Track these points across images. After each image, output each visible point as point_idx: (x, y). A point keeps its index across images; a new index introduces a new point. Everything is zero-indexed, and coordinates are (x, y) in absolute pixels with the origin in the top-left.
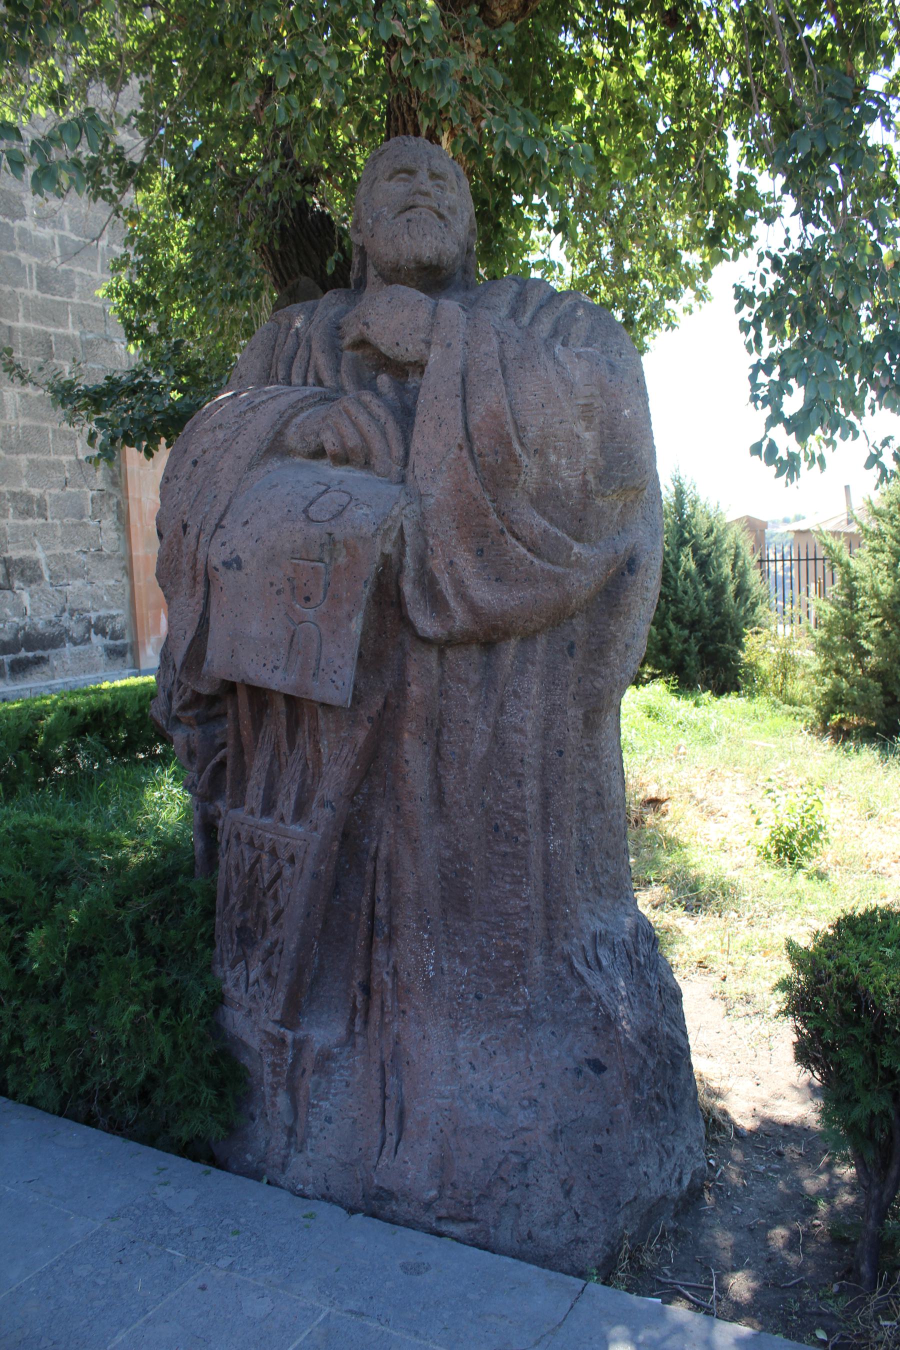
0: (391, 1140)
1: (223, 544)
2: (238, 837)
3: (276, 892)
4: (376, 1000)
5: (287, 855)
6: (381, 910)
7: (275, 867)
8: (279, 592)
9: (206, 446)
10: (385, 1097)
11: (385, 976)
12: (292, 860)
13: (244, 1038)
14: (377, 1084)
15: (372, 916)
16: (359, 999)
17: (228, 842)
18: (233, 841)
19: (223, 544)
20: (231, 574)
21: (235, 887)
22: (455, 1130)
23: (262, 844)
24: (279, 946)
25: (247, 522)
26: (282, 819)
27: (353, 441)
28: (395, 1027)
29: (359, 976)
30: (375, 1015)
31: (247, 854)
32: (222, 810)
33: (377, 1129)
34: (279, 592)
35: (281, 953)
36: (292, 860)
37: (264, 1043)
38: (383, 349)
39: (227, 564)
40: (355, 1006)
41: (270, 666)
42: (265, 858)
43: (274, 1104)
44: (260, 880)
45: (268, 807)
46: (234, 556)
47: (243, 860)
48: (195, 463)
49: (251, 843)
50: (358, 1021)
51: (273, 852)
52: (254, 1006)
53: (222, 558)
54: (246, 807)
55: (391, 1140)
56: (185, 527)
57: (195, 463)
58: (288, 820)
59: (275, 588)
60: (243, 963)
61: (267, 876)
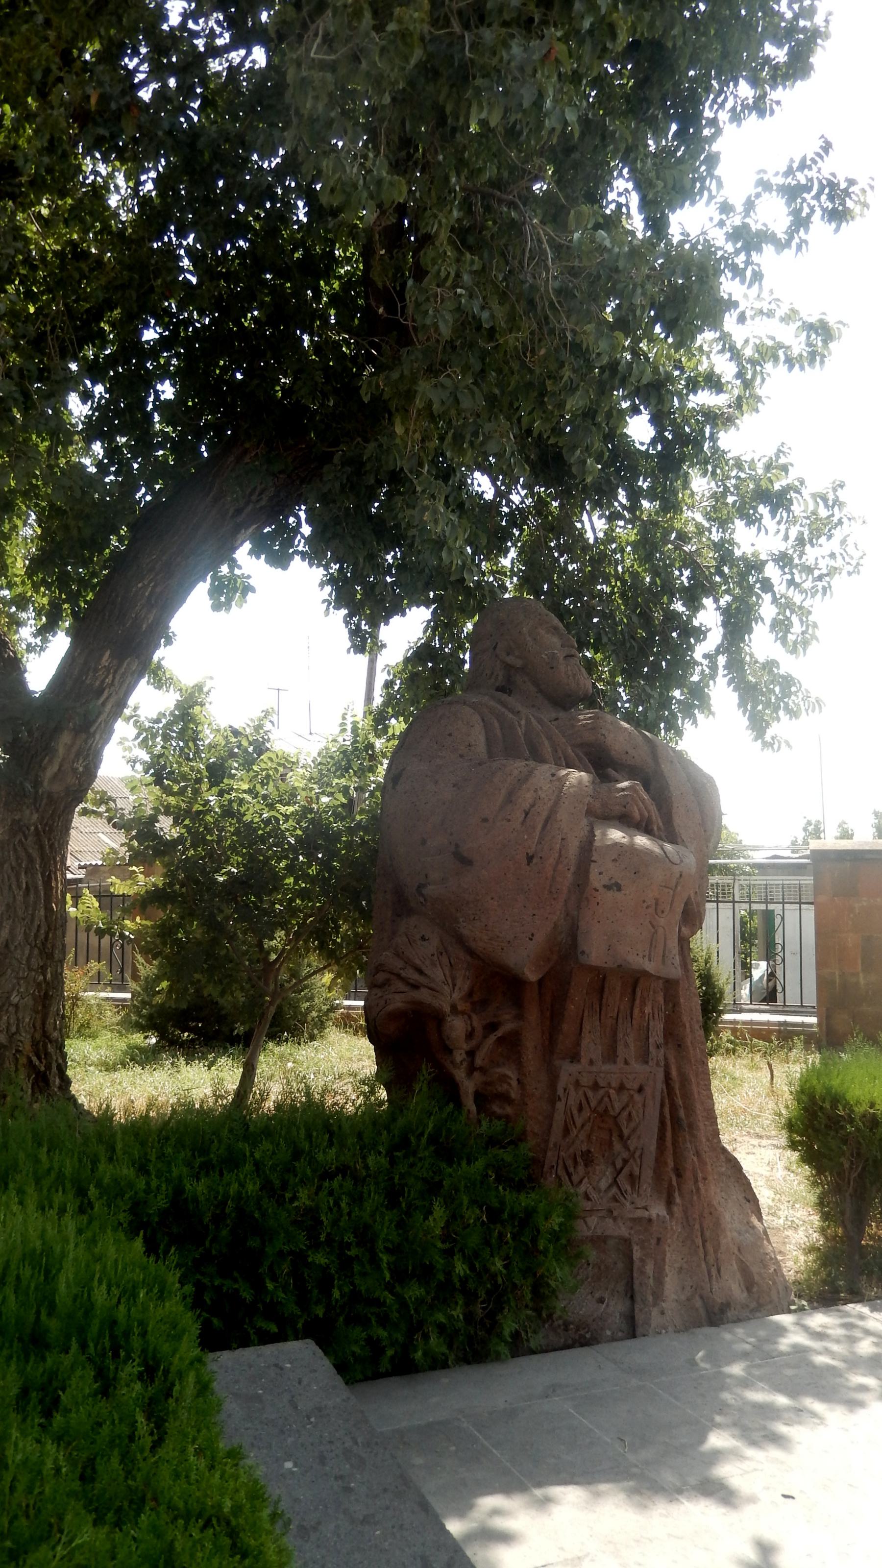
0: (714, 1271)
1: (600, 873)
2: (577, 1084)
3: (630, 1114)
4: (688, 1174)
5: (636, 1086)
6: (682, 1113)
7: (625, 1098)
8: (648, 907)
9: (531, 801)
10: (704, 1242)
11: (695, 1159)
12: (640, 1090)
13: (608, 1233)
14: (699, 1234)
15: (675, 1120)
16: (674, 1179)
17: (565, 1090)
18: (571, 1088)
19: (600, 873)
20: (610, 894)
21: (579, 1122)
22: (739, 1250)
23: (609, 1084)
24: (637, 1154)
25: (615, 860)
26: (626, 1062)
27: (646, 814)
28: (703, 1191)
29: (671, 1163)
30: (689, 1185)
31: (590, 1094)
32: (509, 1073)
33: (704, 1265)
34: (648, 907)
35: (641, 1156)
36: (640, 1090)
37: (631, 1228)
38: (613, 753)
39: (607, 887)
40: (670, 1185)
41: (641, 955)
42: (612, 1091)
43: (643, 1273)
44: (609, 1108)
45: (611, 1055)
46: (613, 881)
47: (587, 1099)
48: (527, 814)
49: (596, 1086)
50: (677, 1194)
51: (621, 1088)
52: (613, 1205)
53: (603, 883)
54: (584, 1061)
55: (714, 1271)
56: (530, 859)
57: (527, 814)
58: (633, 1062)
59: (645, 905)
60: (586, 1180)
61: (618, 1106)
